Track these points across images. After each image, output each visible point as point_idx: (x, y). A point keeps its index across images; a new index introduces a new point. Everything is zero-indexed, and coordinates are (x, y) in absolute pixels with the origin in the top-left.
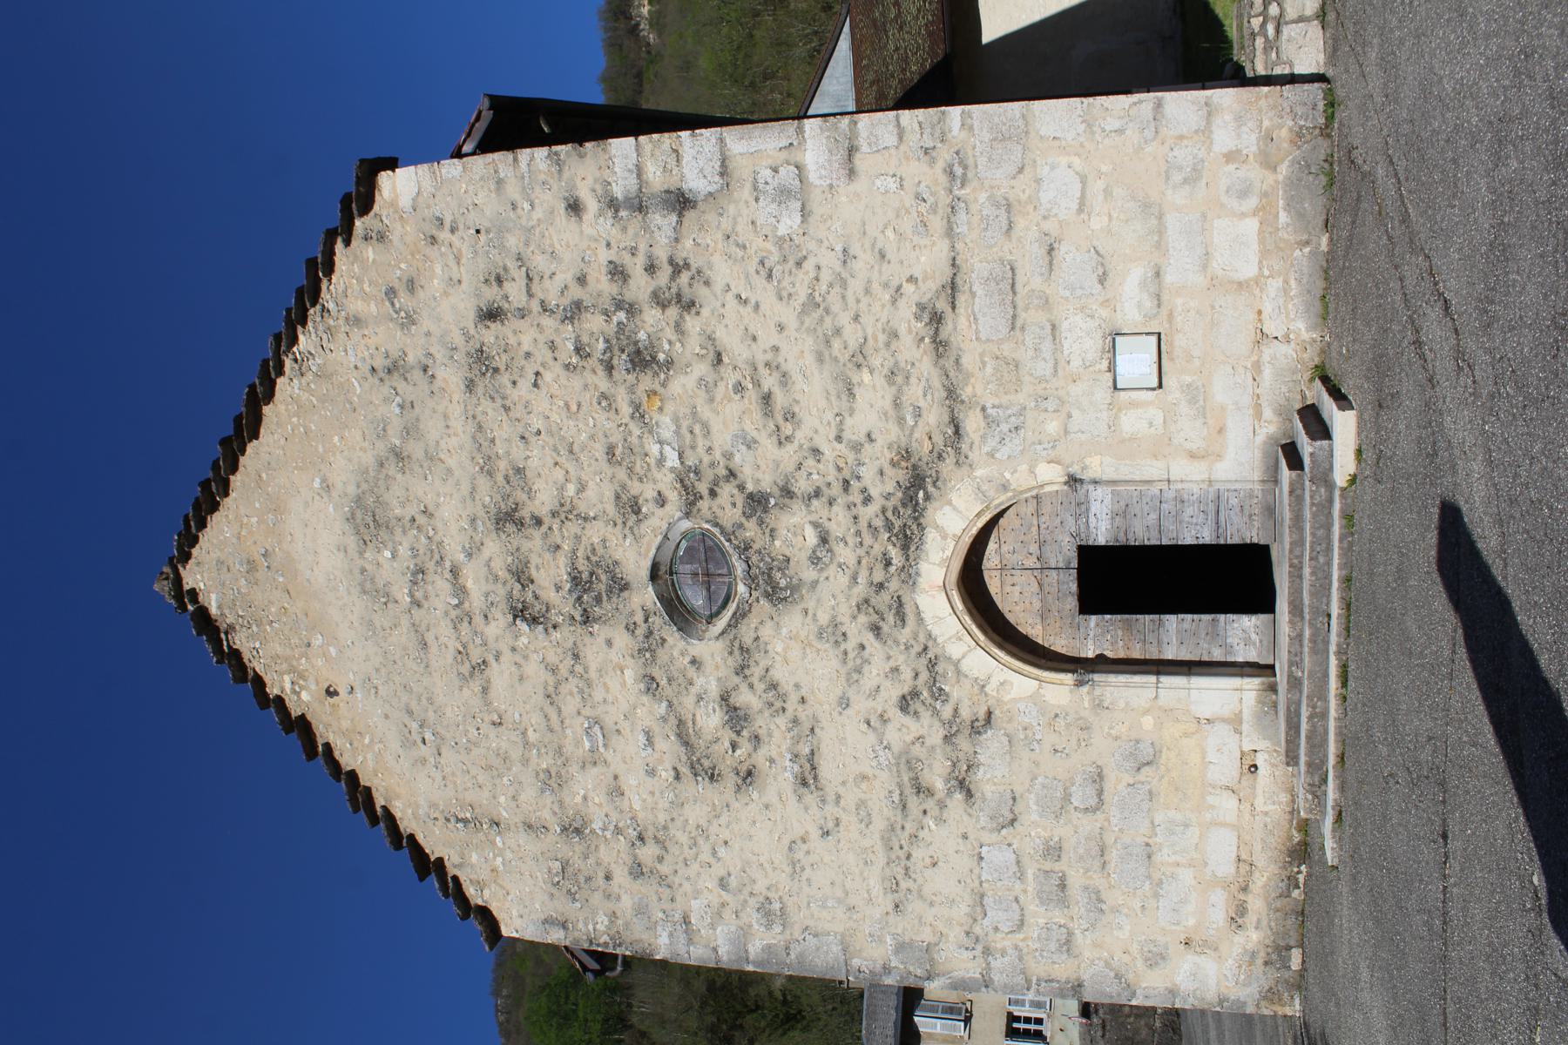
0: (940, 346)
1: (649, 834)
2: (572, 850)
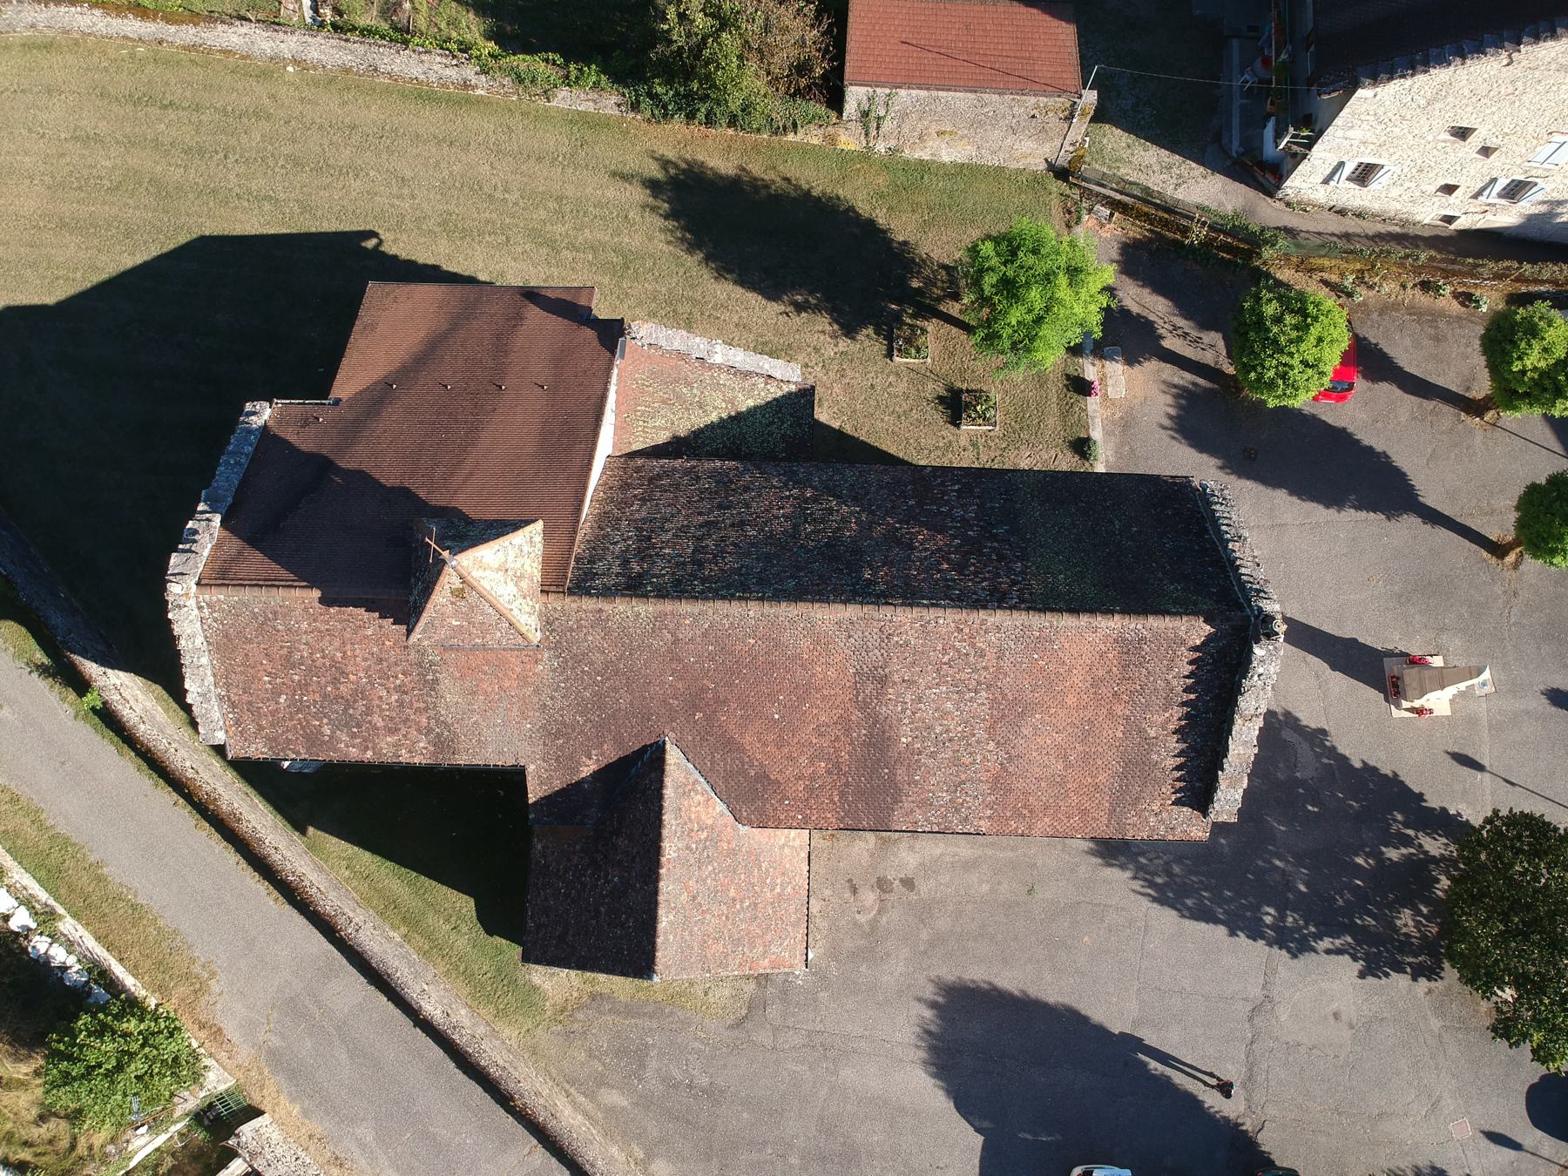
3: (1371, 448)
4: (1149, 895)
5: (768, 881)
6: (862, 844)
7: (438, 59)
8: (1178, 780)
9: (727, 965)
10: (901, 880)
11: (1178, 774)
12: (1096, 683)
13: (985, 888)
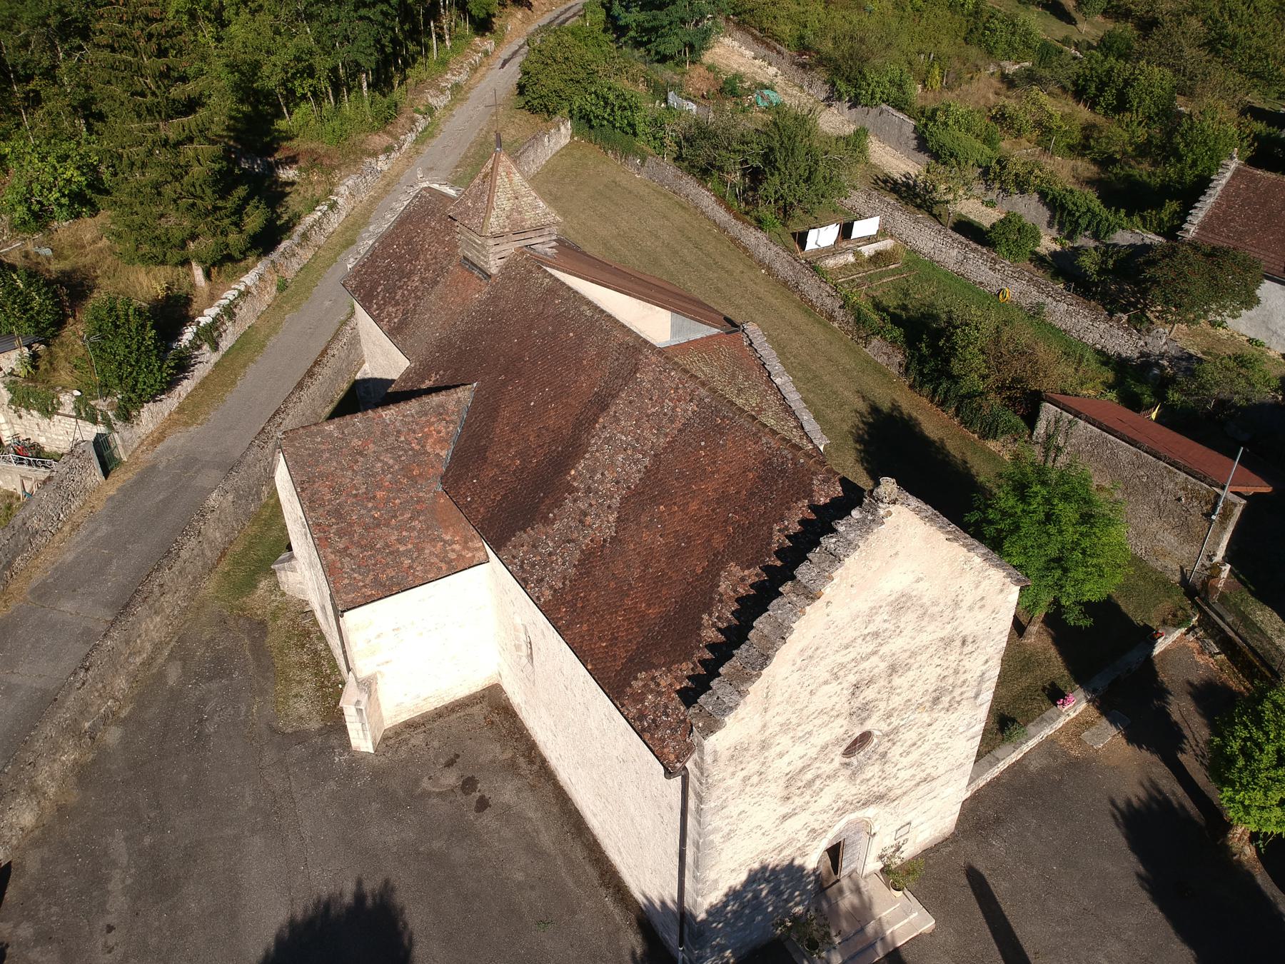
0: (918, 784)
1: (763, 776)
2: (754, 748)
5: (404, 533)
6: (498, 749)
7: (828, 288)
9: (314, 510)
10: (482, 797)
12: (723, 498)
13: (520, 876)
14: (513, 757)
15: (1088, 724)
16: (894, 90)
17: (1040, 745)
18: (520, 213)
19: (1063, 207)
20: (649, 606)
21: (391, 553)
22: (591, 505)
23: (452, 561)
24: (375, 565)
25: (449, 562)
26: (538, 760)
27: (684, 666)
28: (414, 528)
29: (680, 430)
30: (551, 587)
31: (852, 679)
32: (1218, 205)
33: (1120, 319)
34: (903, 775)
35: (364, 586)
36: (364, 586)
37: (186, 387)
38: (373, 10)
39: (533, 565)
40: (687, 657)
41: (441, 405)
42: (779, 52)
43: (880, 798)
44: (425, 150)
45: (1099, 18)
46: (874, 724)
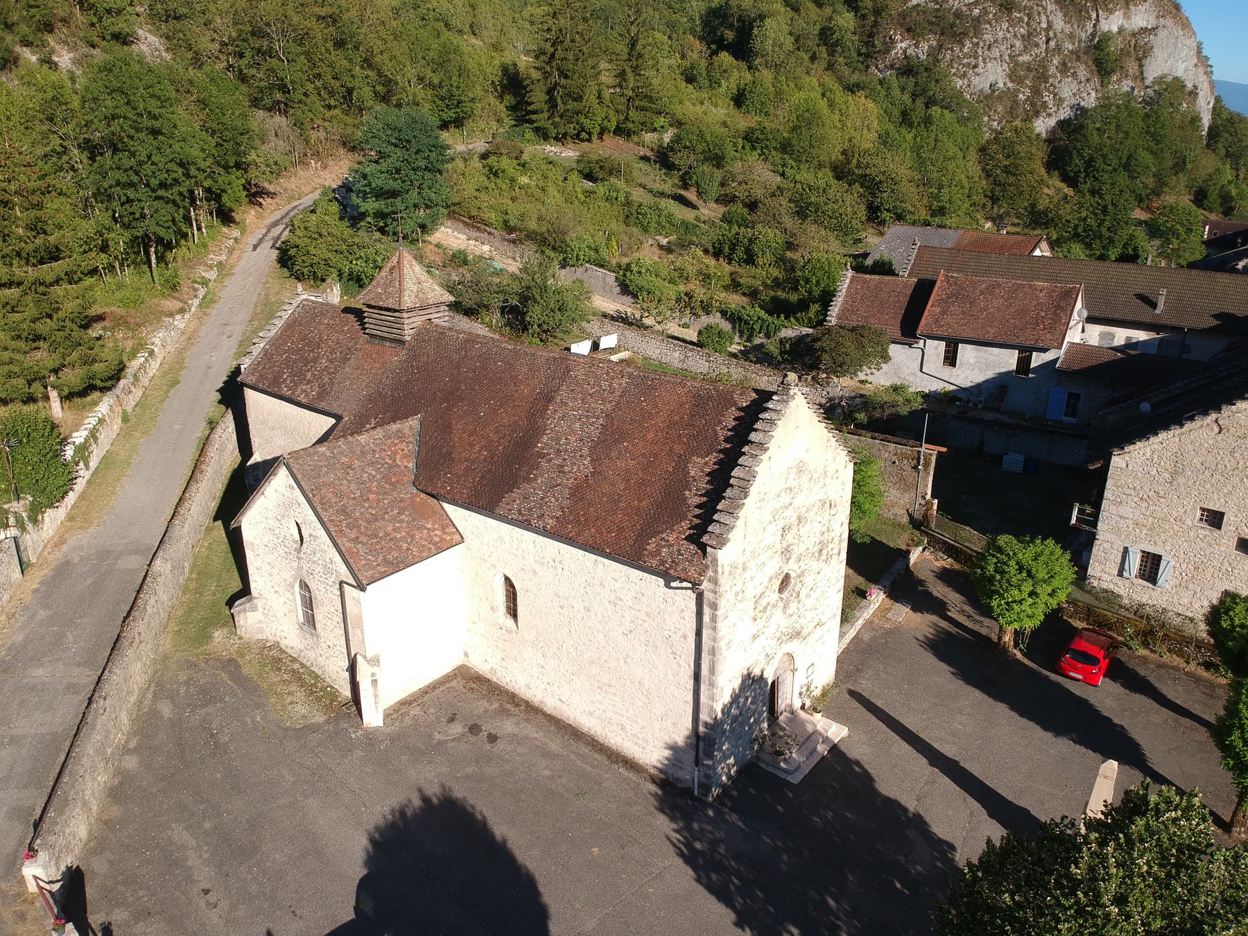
0: (815, 627)
3: (1109, 720)
4: (679, 849)
6: (486, 704)
8: (696, 517)
11: (698, 511)
12: (672, 424)
13: (547, 773)
14: (501, 705)
15: (889, 609)
16: (592, 253)
17: (864, 626)
18: (424, 293)
19: (740, 319)
20: (640, 501)
21: (391, 540)
22: (565, 459)
23: (437, 543)
24: (382, 549)
25: (435, 544)
26: (522, 703)
27: (683, 524)
28: (402, 521)
29: (621, 396)
30: (552, 517)
31: (781, 523)
32: (845, 302)
33: (807, 379)
34: (809, 615)
35: (378, 565)
36: (378, 565)
37: (71, 498)
38: (170, 192)
39: (530, 509)
40: (684, 518)
41: (399, 431)
42: (490, 233)
43: (796, 635)
44: (213, 311)
45: (713, 205)
46: (793, 568)
